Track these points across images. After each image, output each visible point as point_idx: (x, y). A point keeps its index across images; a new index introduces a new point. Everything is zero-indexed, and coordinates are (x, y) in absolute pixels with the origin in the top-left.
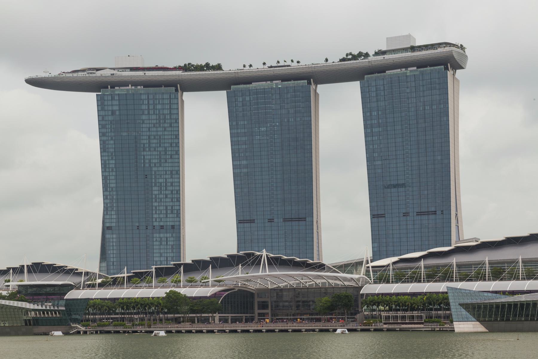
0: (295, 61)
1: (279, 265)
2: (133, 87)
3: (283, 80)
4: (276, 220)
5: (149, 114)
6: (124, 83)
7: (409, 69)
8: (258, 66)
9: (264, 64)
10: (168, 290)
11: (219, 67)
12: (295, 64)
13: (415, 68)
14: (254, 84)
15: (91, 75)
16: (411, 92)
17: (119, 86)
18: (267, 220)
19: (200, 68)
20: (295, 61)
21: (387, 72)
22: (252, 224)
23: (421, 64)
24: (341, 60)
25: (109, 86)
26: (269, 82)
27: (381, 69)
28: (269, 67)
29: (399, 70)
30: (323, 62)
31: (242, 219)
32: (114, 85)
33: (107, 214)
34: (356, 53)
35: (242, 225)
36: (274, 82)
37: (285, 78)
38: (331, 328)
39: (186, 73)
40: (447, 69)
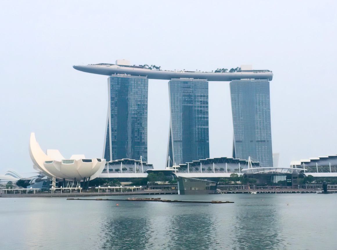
1: (231, 163)
2: (126, 75)
5: (134, 88)
10: (231, 173)
12: (198, 71)
13: (254, 79)
14: (181, 78)
15: (108, 67)
17: (120, 74)
23: (257, 78)
24: (216, 71)
25: (115, 74)
26: (188, 78)
27: (239, 78)
28: (185, 72)
32: (118, 72)
36: (190, 78)
37: (196, 77)
38: (249, 192)
40: (268, 80)
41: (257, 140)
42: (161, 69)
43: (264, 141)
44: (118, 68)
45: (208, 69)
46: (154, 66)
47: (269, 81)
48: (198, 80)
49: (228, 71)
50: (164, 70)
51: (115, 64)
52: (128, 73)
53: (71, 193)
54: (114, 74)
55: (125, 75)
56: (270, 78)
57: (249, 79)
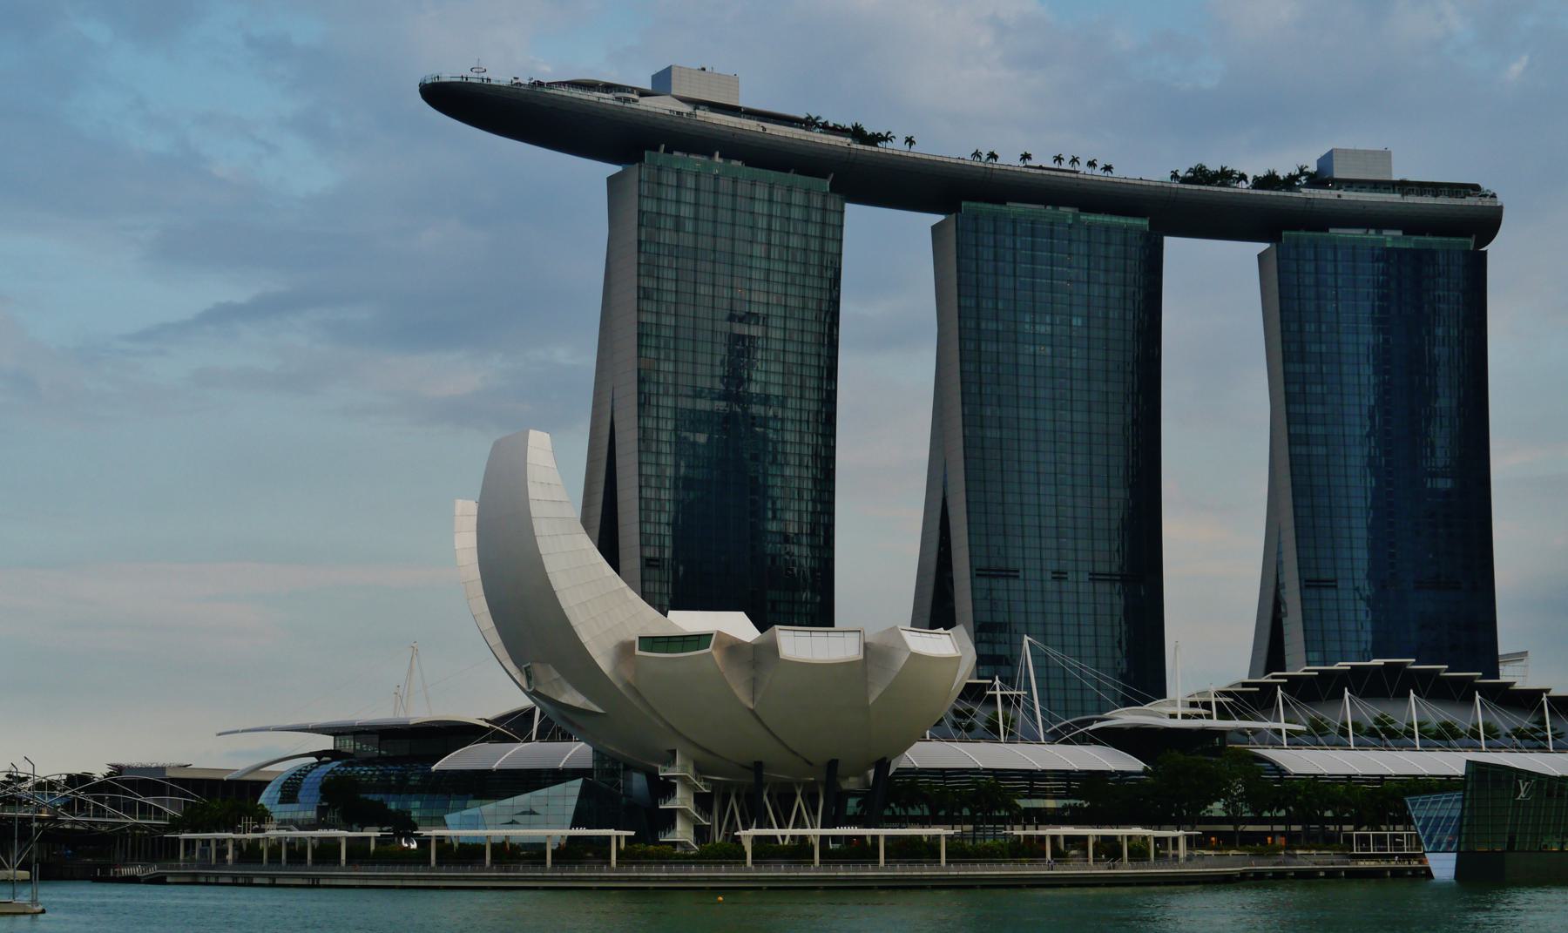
0: (1100, 165)
4: (1070, 576)
7: (1385, 232)
8: (1009, 159)
9: (1026, 157)
13: (1399, 233)
16: (1387, 290)
18: (1049, 576)
20: (1100, 165)
22: (1011, 581)
23: (1412, 223)
27: (1320, 219)
30: (1167, 177)
31: (984, 564)
33: (648, 521)
34: (1213, 166)
35: (984, 582)
45: (1149, 163)
53: (816, 869)
54: (657, 149)
57: (1372, 232)
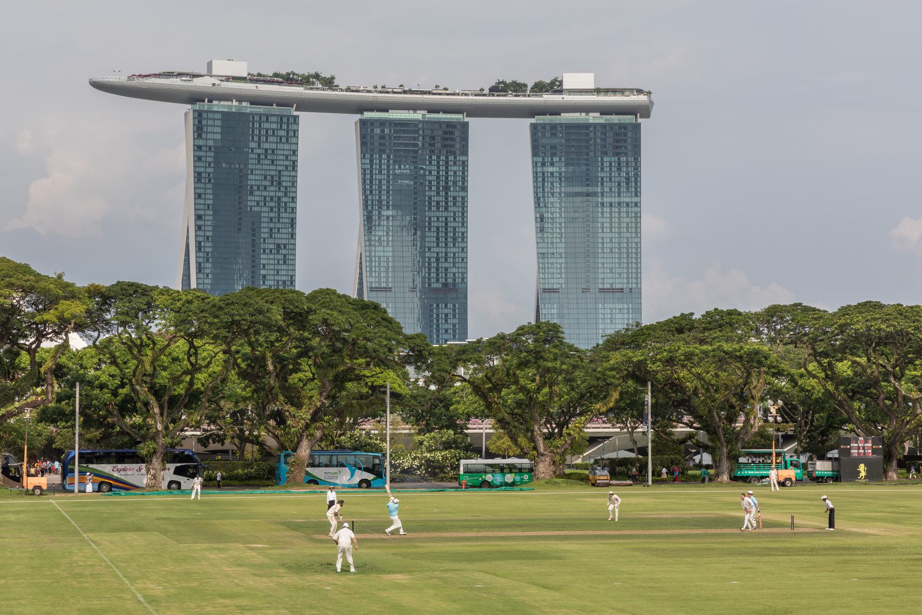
0: (441, 88)
2: (237, 104)
3: (430, 111)
6: (227, 97)
7: (591, 114)
11: (329, 83)
13: (598, 115)
15: (189, 84)
18: (407, 290)
19: (305, 81)
20: (441, 88)
21: (562, 114)
24: (494, 90)
27: (555, 110)
29: (578, 114)
39: (307, 91)
41: (601, 286)
42: (336, 82)
43: (621, 290)
44: (214, 84)
46: (317, 76)
47: (641, 117)
48: (441, 116)
49: (529, 88)
50: (344, 87)
51: (205, 72)
52: (240, 99)
55: (235, 103)
56: (644, 111)
57: (583, 114)
